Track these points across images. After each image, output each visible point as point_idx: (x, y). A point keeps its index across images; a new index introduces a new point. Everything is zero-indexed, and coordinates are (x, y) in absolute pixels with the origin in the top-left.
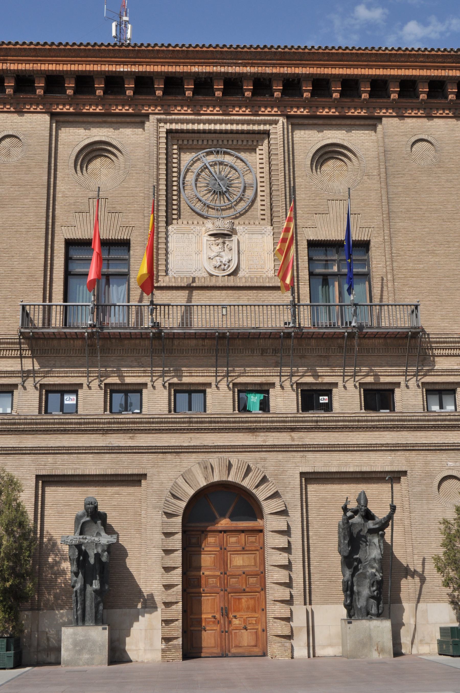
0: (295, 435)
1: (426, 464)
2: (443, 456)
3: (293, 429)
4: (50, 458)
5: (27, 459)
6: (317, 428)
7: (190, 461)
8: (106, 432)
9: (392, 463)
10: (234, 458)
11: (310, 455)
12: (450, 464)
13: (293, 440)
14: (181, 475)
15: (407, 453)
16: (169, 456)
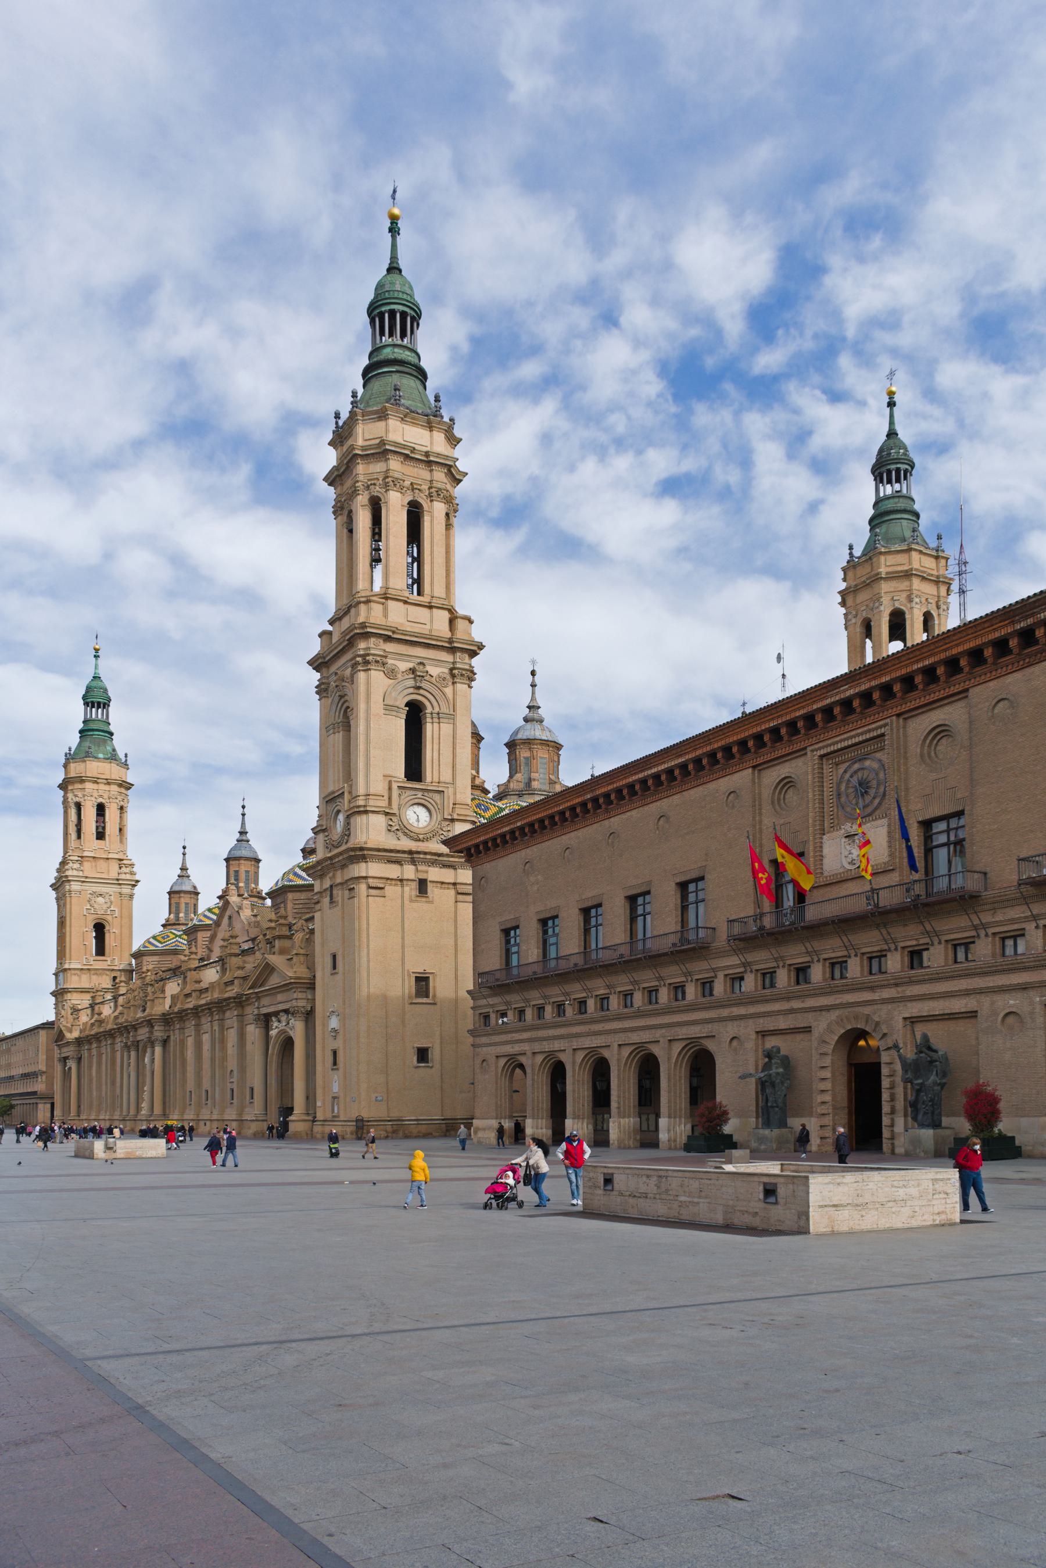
0: (899, 989)
1: (993, 1003)
2: (1007, 996)
3: (897, 985)
4: (761, 1020)
5: (751, 1021)
6: (911, 982)
7: (834, 1015)
8: (788, 999)
9: (966, 1004)
10: (860, 1009)
11: (909, 1004)
12: (1012, 1002)
13: (898, 993)
14: (827, 1028)
15: (978, 996)
16: (824, 1013)
